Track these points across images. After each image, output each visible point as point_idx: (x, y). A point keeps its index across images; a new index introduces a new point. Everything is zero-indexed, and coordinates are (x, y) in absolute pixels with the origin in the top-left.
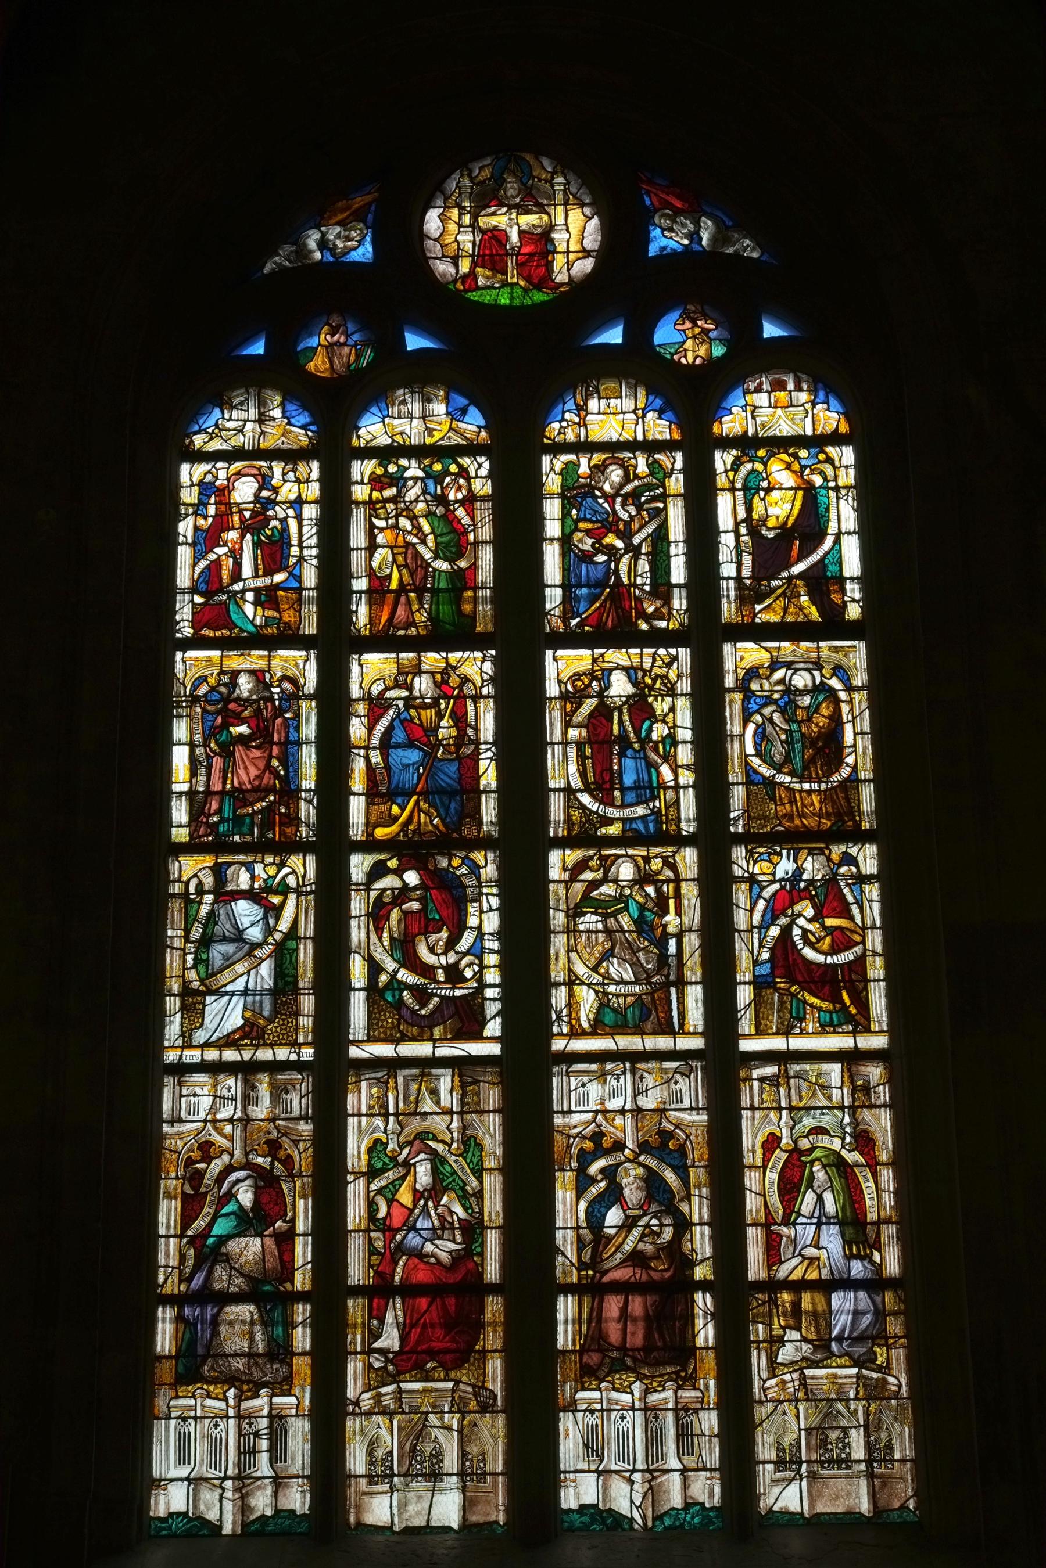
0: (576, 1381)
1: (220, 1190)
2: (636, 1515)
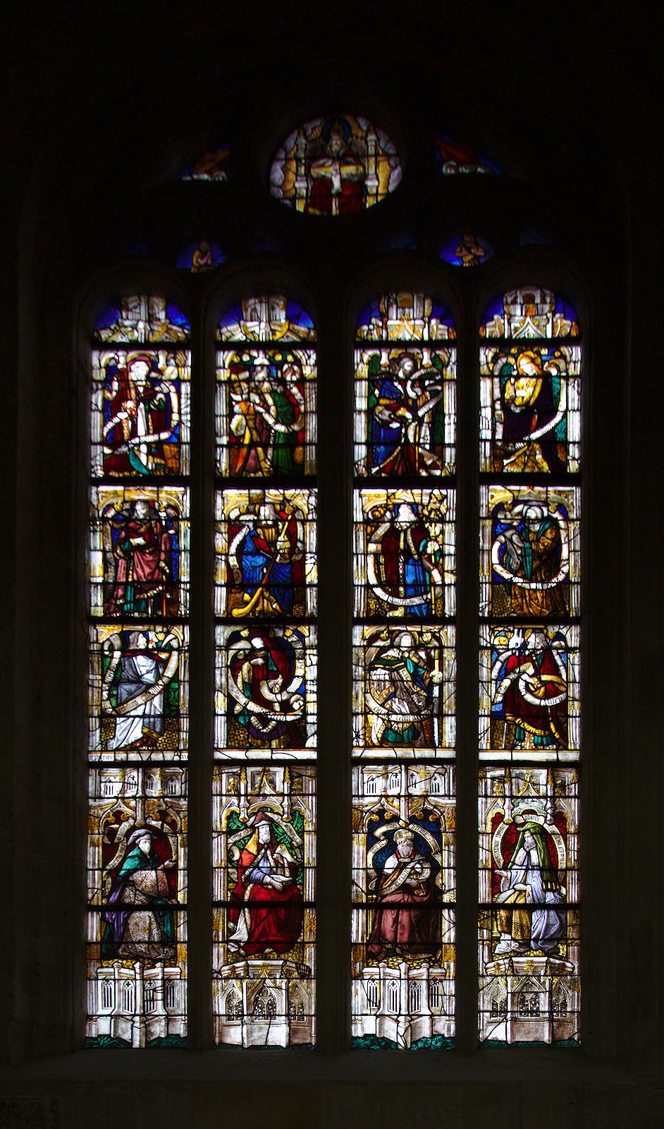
0: (363, 961)
1: (127, 841)
2: (400, 1041)
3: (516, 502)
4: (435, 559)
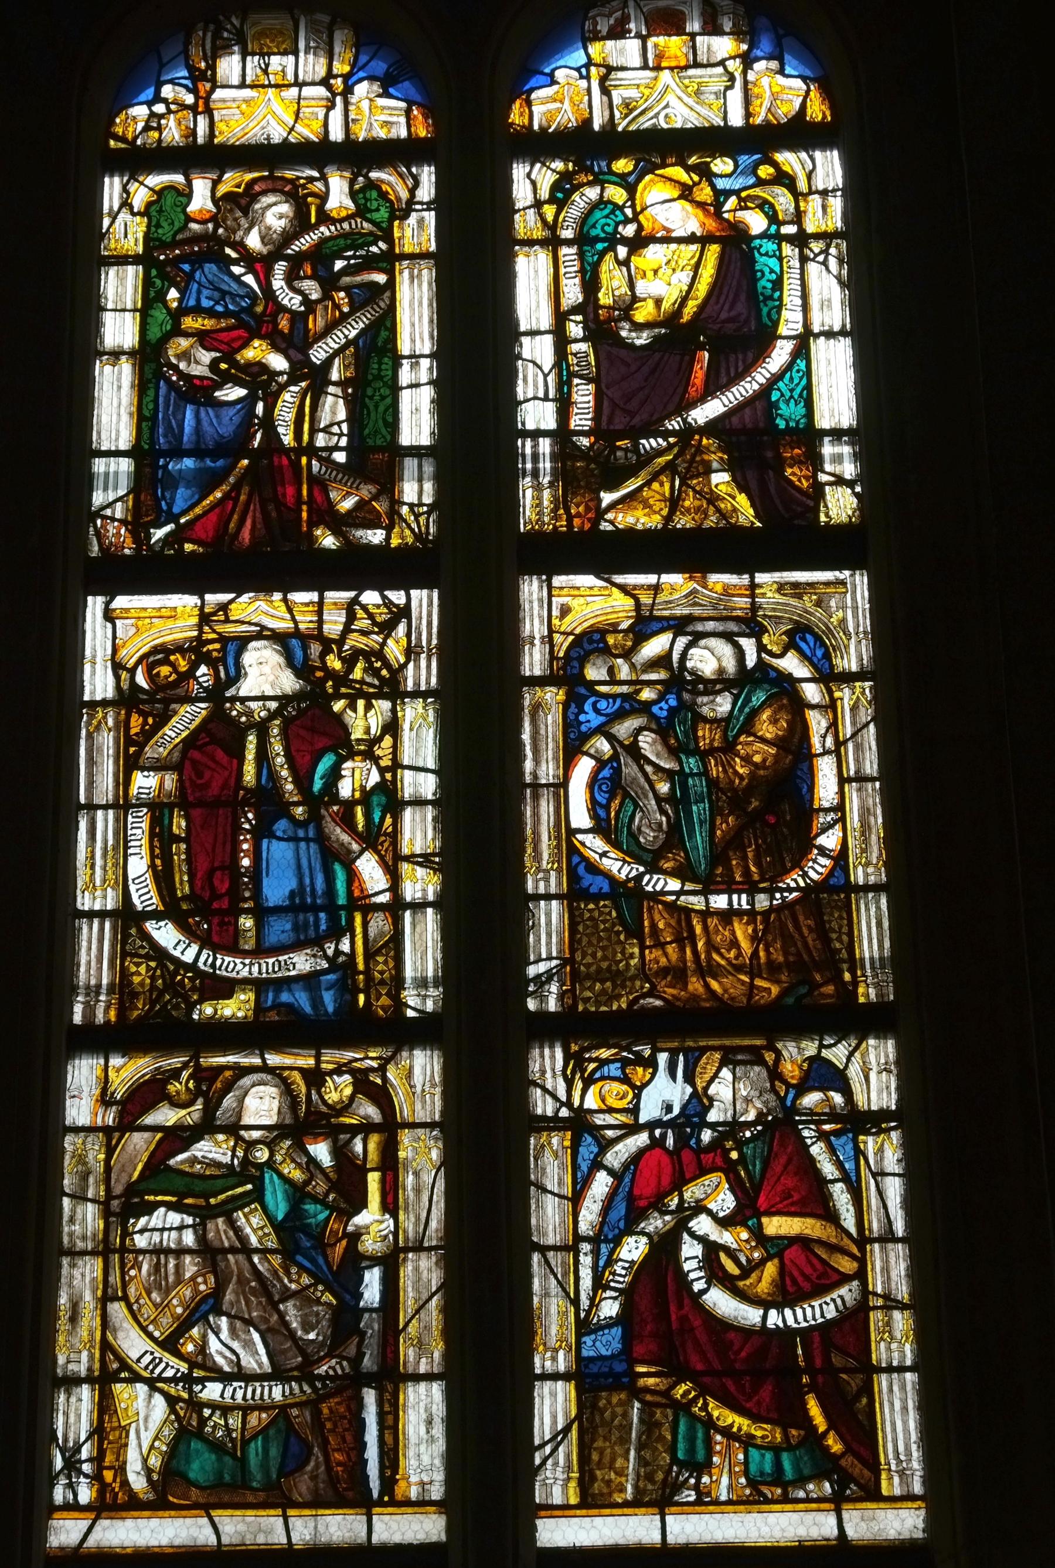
3: (645, 625)
4: (368, 815)
